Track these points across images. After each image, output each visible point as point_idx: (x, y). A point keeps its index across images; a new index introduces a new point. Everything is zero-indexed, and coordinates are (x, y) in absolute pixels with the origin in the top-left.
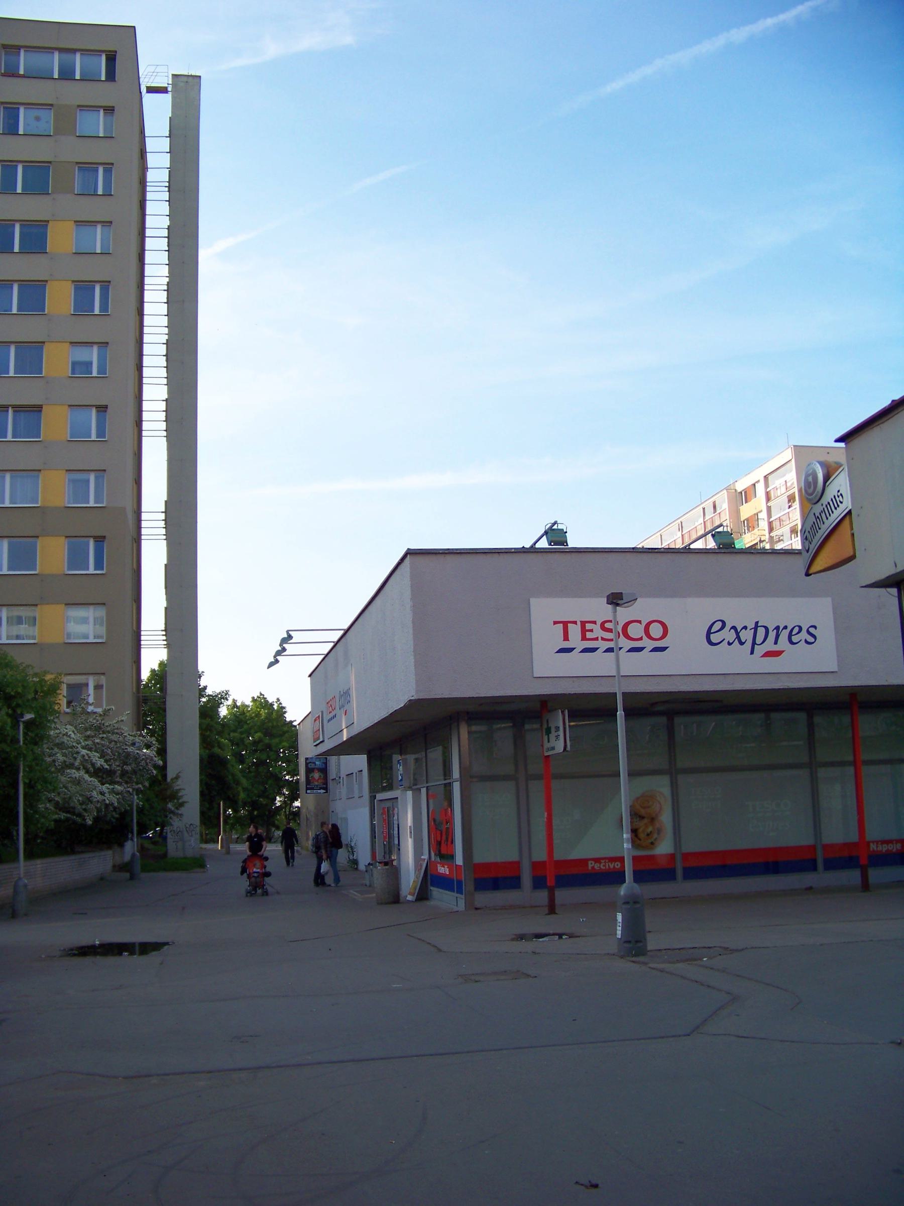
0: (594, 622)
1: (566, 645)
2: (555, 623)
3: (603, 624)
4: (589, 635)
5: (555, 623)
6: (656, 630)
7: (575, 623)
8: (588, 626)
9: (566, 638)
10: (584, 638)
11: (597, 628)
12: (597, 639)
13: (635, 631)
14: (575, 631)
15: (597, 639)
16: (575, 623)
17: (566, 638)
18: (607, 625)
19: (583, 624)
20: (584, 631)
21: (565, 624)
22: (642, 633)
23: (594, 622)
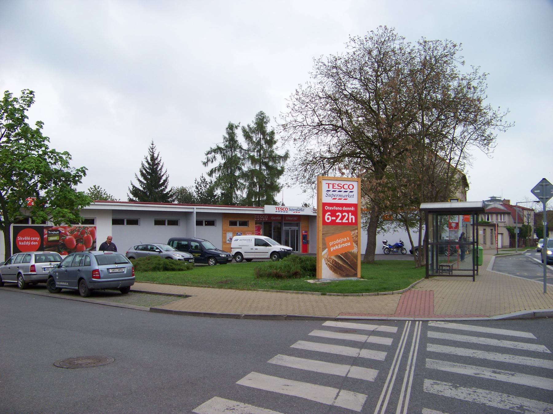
0: (336, 184)
1: (329, 189)
2: (326, 183)
3: (338, 185)
4: (334, 187)
5: (326, 183)
6: (351, 187)
7: (331, 184)
8: (334, 185)
9: (329, 188)
10: (333, 188)
11: (336, 185)
12: (336, 188)
13: (346, 187)
14: (331, 186)
15: (336, 188)
16: (331, 184)
17: (329, 188)
18: (339, 185)
19: (333, 184)
20: (333, 186)
21: (329, 184)
22: (348, 188)
23: (336, 184)
